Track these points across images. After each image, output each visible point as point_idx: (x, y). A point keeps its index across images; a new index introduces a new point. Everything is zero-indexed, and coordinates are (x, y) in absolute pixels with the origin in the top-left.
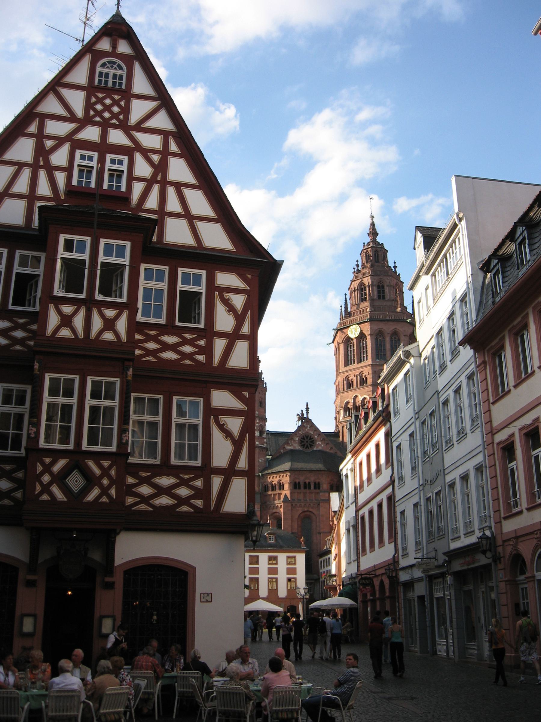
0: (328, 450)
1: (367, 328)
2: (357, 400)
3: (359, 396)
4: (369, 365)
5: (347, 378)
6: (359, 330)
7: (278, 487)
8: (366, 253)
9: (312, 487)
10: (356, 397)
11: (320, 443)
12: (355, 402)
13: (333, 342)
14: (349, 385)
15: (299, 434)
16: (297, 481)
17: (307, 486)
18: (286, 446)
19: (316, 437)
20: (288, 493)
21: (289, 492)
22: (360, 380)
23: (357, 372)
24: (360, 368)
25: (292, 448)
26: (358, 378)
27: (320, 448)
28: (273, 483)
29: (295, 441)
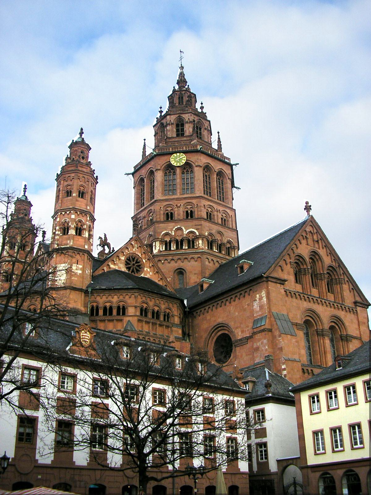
0: (157, 281)
3: (183, 228)
6: (185, 159)
7: (115, 312)
9: (162, 318)
11: (149, 270)
13: (133, 174)
14: (170, 217)
15: (126, 252)
16: (145, 306)
17: (156, 315)
18: (110, 264)
19: (144, 261)
20: (134, 320)
21: (136, 318)
22: (183, 212)
24: (185, 198)
25: (116, 268)
27: (148, 276)
28: (108, 305)
29: (119, 259)
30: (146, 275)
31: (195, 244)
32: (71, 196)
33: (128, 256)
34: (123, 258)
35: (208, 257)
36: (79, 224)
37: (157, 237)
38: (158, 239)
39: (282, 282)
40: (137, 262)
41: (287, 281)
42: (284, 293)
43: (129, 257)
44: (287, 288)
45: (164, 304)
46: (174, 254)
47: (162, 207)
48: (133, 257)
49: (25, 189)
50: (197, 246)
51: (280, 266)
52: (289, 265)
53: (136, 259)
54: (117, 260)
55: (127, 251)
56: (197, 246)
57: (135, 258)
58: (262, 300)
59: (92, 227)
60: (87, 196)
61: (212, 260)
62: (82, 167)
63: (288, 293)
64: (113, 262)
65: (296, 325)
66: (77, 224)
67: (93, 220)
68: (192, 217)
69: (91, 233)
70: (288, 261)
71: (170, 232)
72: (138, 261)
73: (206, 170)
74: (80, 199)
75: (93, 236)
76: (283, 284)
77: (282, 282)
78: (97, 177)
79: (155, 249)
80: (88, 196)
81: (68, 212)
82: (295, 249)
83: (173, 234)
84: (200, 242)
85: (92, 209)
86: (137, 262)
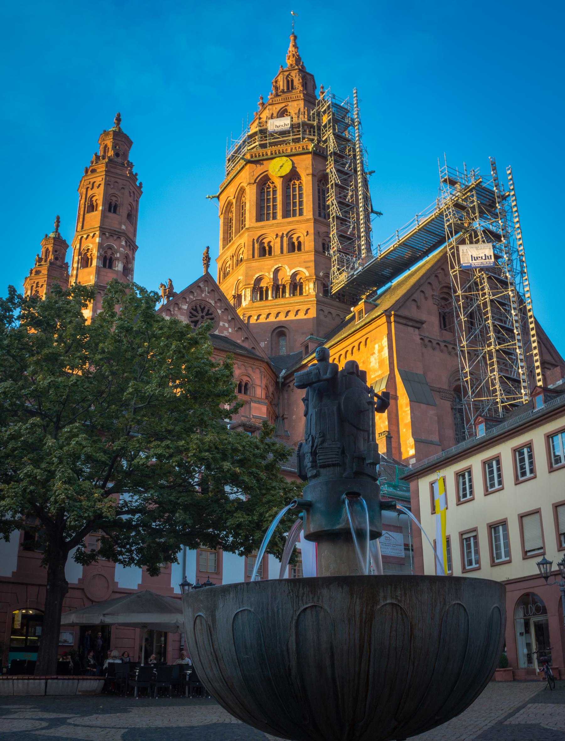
0: (238, 341)
1: (305, 165)
2: (280, 275)
4: (308, 220)
5: (260, 240)
8: (288, 76)
10: (277, 271)
11: (227, 325)
12: (275, 278)
15: (190, 299)
19: (219, 312)
23: (285, 230)
24: (289, 223)
26: (285, 239)
27: (225, 334)
29: (180, 309)
30: (223, 333)
31: (304, 290)
32: (96, 210)
33: (193, 304)
34: (185, 307)
35: (323, 308)
36: (109, 252)
37: (247, 283)
38: (250, 284)
39: (418, 324)
40: (208, 314)
41: (425, 322)
42: (420, 341)
43: (196, 307)
44: (427, 334)
45: (239, 368)
46: (271, 306)
47: (256, 239)
48: (202, 307)
49: (58, 221)
50: (307, 292)
51: (414, 300)
52: (430, 302)
53: (206, 309)
54: (176, 309)
55: (192, 297)
56: (307, 292)
57: (204, 308)
58: (382, 351)
59: (131, 256)
60: (121, 211)
61: (330, 313)
62: (115, 168)
63: (426, 342)
64: (169, 312)
65: (439, 391)
66: (106, 252)
67: (133, 247)
68: (299, 249)
69: (130, 266)
70: (429, 292)
71: (267, 274)
72: (210, 312)
73: (323, 181)
74: (111, 215)
75: (133, 271)
76: (419, 328)
77: (418, 324)
78: (141, 184)
79: (245, 300)
80: (123, 211)
81: (91, 235)
82: (441, 276)
83: (272, 276)
84: (311, 285)
85: (132, 231)
86: (208, 314)
